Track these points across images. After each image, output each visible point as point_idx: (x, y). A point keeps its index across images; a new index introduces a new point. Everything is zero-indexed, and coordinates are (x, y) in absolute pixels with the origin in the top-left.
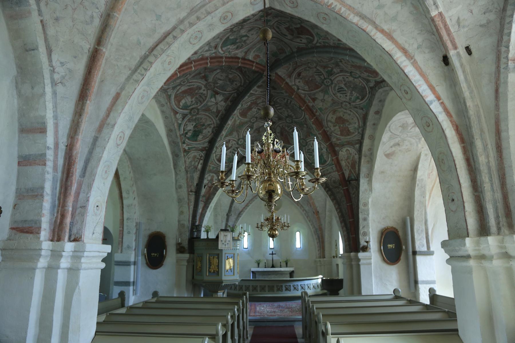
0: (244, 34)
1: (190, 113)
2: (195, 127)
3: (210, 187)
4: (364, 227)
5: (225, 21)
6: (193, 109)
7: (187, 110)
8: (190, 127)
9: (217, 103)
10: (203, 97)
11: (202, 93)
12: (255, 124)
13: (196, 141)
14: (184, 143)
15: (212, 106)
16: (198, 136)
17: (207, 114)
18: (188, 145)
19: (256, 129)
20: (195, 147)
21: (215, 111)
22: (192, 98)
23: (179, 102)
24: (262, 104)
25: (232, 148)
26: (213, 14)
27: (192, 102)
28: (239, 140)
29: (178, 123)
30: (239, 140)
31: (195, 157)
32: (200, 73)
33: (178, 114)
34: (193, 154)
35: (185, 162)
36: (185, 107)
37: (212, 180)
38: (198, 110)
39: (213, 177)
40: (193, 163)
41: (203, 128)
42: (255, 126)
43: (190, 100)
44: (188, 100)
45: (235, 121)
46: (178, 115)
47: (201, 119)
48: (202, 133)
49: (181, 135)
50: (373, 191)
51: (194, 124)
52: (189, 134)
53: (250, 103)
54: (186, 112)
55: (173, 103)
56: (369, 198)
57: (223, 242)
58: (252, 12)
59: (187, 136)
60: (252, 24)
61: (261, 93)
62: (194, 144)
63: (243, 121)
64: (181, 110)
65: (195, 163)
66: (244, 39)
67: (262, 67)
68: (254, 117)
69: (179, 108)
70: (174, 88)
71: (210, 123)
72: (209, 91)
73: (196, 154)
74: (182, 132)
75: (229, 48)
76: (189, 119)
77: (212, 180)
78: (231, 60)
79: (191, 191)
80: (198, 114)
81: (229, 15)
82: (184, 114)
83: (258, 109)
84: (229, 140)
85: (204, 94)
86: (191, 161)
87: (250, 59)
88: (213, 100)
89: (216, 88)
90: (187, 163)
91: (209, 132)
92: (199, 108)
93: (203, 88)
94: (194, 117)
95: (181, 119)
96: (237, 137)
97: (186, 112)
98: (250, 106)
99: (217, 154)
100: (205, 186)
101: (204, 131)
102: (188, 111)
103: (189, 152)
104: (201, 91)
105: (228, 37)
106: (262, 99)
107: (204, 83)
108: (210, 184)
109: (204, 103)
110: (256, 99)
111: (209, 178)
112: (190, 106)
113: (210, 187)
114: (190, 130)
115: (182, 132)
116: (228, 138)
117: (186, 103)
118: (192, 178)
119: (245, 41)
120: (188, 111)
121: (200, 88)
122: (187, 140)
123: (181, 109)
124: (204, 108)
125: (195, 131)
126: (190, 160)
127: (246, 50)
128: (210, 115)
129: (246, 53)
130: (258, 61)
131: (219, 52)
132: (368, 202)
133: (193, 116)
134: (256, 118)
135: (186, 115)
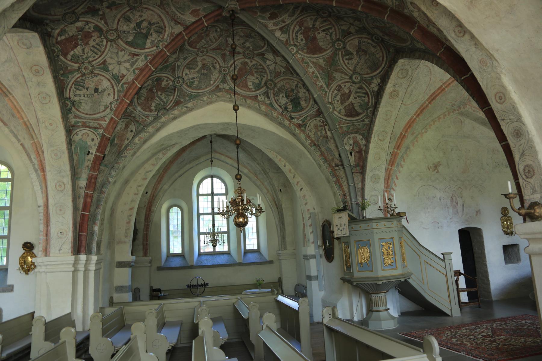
0: (132, 25)
1: (268, 88)
2: (287, 97)
3: (360, 152)
4: (522, 154)
5: (42, 73)
6: (266, 83)
7: (263, 87)
8: (284, 100)
9: (275, 63)
10: (259, 67)
11: (254, 65)
12: (347, 46)
13: (303, 109)
14: (292, 118)
15: (275, 68)
16: (299, 103)
17: (282, 78)
18: (298, 119)
19: (357, 52)
20: (307, 116)
21: (283, 70)
22: (253, 76)
23: (246, 86)
24: (318, 23)
25: (353, 92)
26: (27, 80)
27: (257, 78)
28: (351, 78)
29: (266, 105)
30: (351, 78)
31: (316, 126)
32: (223, 56)
33: (259, 97)
34: (311, 124)
35: (309, 137)
36: (258, 87)
37: (356, 143)
38: (271, 80)
39: (354, 138)
40: (319, 133)
41: (295, 92)
42: (351, 50)
43: (254, 78)
44: (252, 80)
45: (313, 63)
46: (259, 98)
47: (284, 86)
48: (300, 98)
49: (282, 114)
50: (496, 55)
51: (283, 94)
52: (290, 107)
53: (300, 36)
54: (263, 90)
55: (242, 92)
56: (499, 78)
57: (339, 227)
58: (41, 48)
59: (289, 110)
60: (109, 21)
61: (293, 18)
62: (303, 114)
63: (327, 56)
64: (258, 92)
65: (321, 133)
66: (145, 24)
67: (216, 13)
68: (334, 42)
69: (253, 91)
70: (224, 81)
71: (295, 83)
72: (255, 59)
73: (315, 122)
74: (281, 110)
75: (152, 42)
76: (274, 94)
77: (356, 143)
78: (173, 43)
79: (337, 166)
80: (275, 84)
81: (34, 68)
82: (264, 93)
83: (324, 31)
84: (340, 86)
85: (257, 64)
86: (316, 133)
87: (194, 20)
88: (268, 62)
89: (255, 52)
90: (312, 136)
91: (304, 93)
92: (269, 78)
93: (248, 61)
94: (276, 89)
95: (267, 99)
96: (343, 76)
97: (263, 90)
98: (307, 38)
99: (338, 110)
100: (351, 153)
101: (301, 95)
102: (265, 88)
103: (305, 125)
104: (251, 64)
105: (127, 43)
106: (308, 19)
107: (241, 56)
108: (357, 149)
109: (268, 71)
110: (300, 27)
111: (351, 142)
112: (261, 83)
113: (360, 152)
114: (286, 103)
115: (281, 110)
116: (334, 85)
117: (253, 83)
118: (329, 150)
119: (150, 23)
120: (265, 88)
121: (247, 63)
122: (292, 114)
123: (256, 91)
124: (274, 76)
125: (291, 101)
126: (313, 133)
127: (172, 23)
128: (286, 77)
129: (177, 22)
130: (202, 14)
131: (151, 51)
132: (503, 87)
133: (273, 89)
134: (338, 40)
135: (267, 92)
